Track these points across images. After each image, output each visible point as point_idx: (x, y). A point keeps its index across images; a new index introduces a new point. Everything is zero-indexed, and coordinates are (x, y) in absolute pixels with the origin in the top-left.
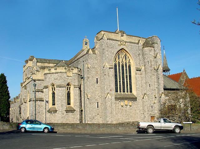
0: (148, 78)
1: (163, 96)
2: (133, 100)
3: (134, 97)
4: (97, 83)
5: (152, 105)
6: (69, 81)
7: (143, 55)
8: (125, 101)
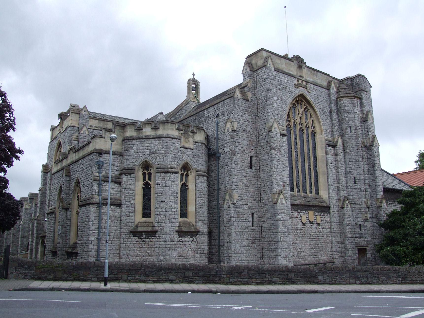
0: (350, 163)
1: (384, 204)
2: (322, 212)
3: (325, 204)
4: (251, 168)
5: (361, 223)
6: (186, 159)
7: (338, 114)
8: (310, 212)
